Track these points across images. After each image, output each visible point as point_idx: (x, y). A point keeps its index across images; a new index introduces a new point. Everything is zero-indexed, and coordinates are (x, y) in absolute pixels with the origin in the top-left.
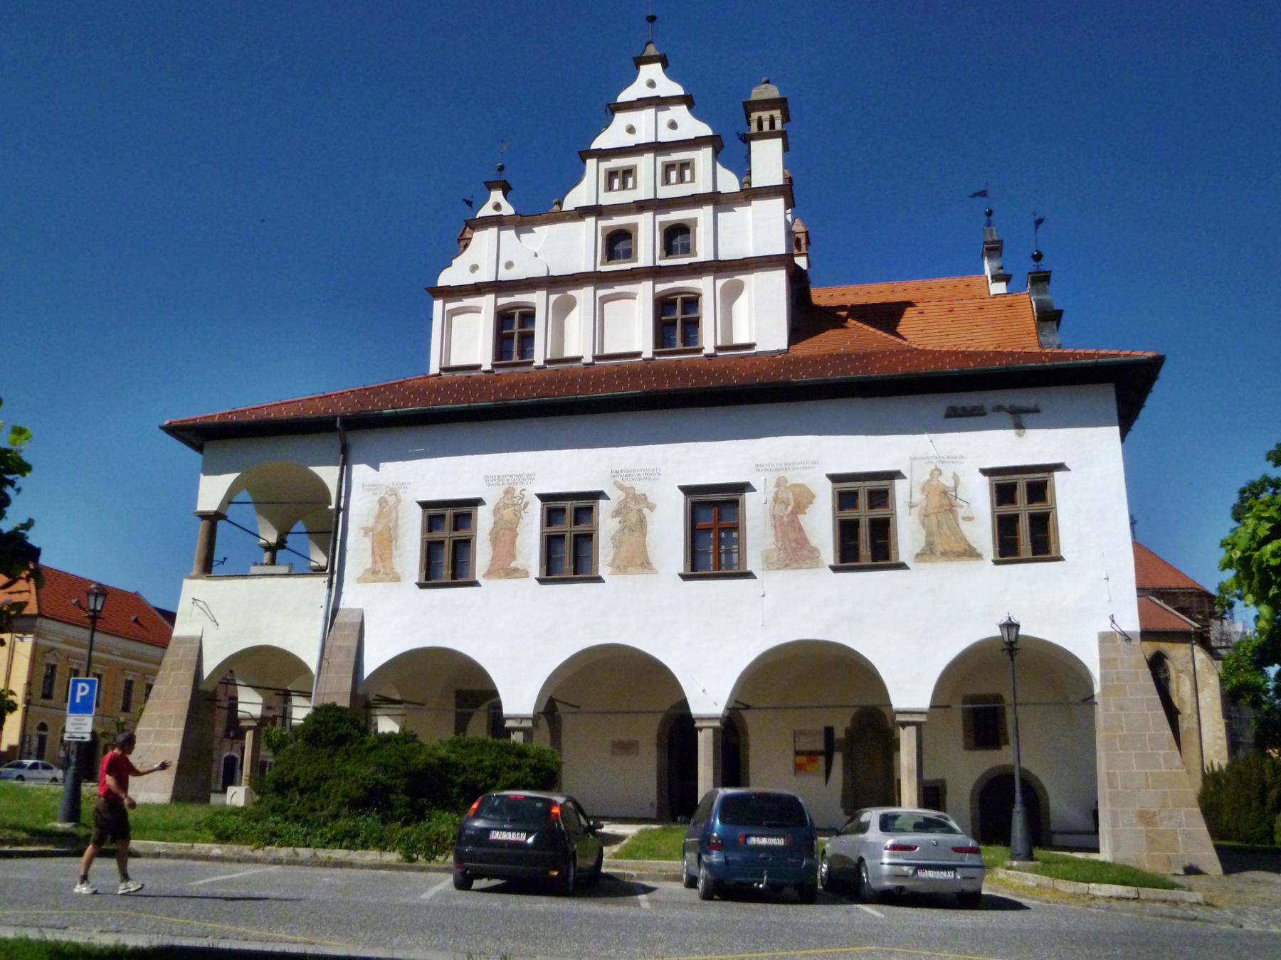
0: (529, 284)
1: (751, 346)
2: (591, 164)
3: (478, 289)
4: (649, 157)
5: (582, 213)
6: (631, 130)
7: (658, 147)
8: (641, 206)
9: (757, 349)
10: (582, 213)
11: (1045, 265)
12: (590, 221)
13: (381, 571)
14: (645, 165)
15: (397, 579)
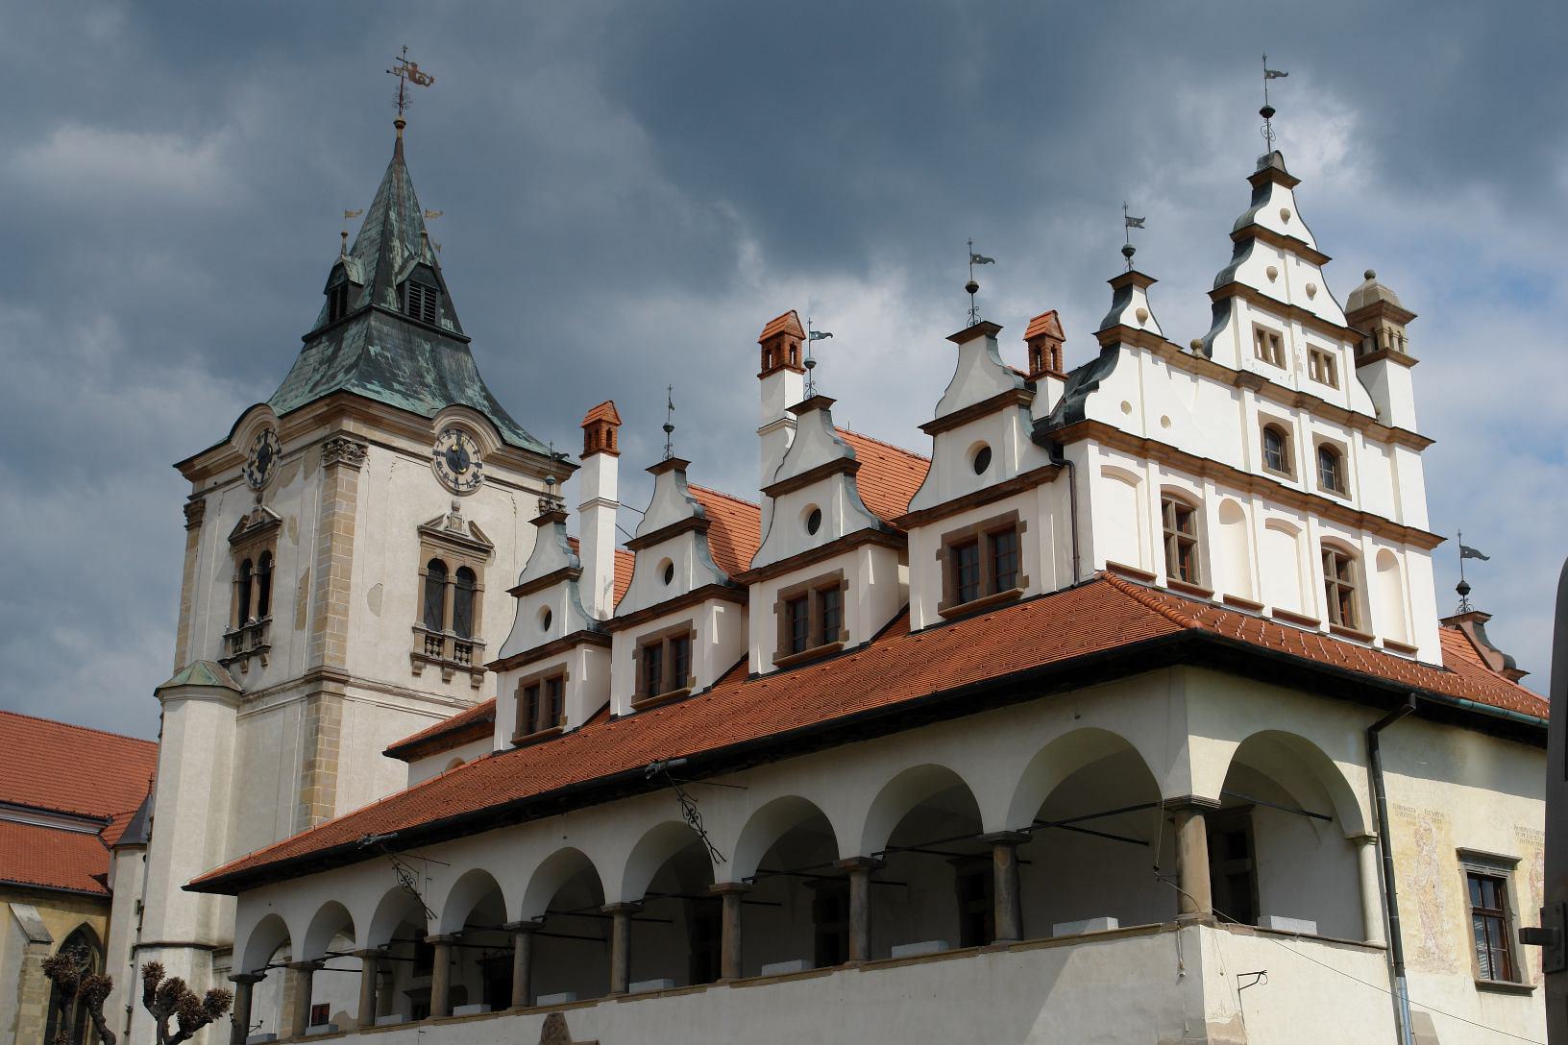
0: (1202, 468)
1: (1412, 651)
2: (1240, 304)
3: (1143, 448)
4: (1297, 328)
5: (1242, 380)
6: (1272, 276)
7: (1310, 320)
8: (1301, 401)
9: (1421, 657)
10: (1242, 380)
11: (1475, 602)
12: (1249, 395)
13: (1435, 959)
14: (1296, 339)
15: (1452, 970)
